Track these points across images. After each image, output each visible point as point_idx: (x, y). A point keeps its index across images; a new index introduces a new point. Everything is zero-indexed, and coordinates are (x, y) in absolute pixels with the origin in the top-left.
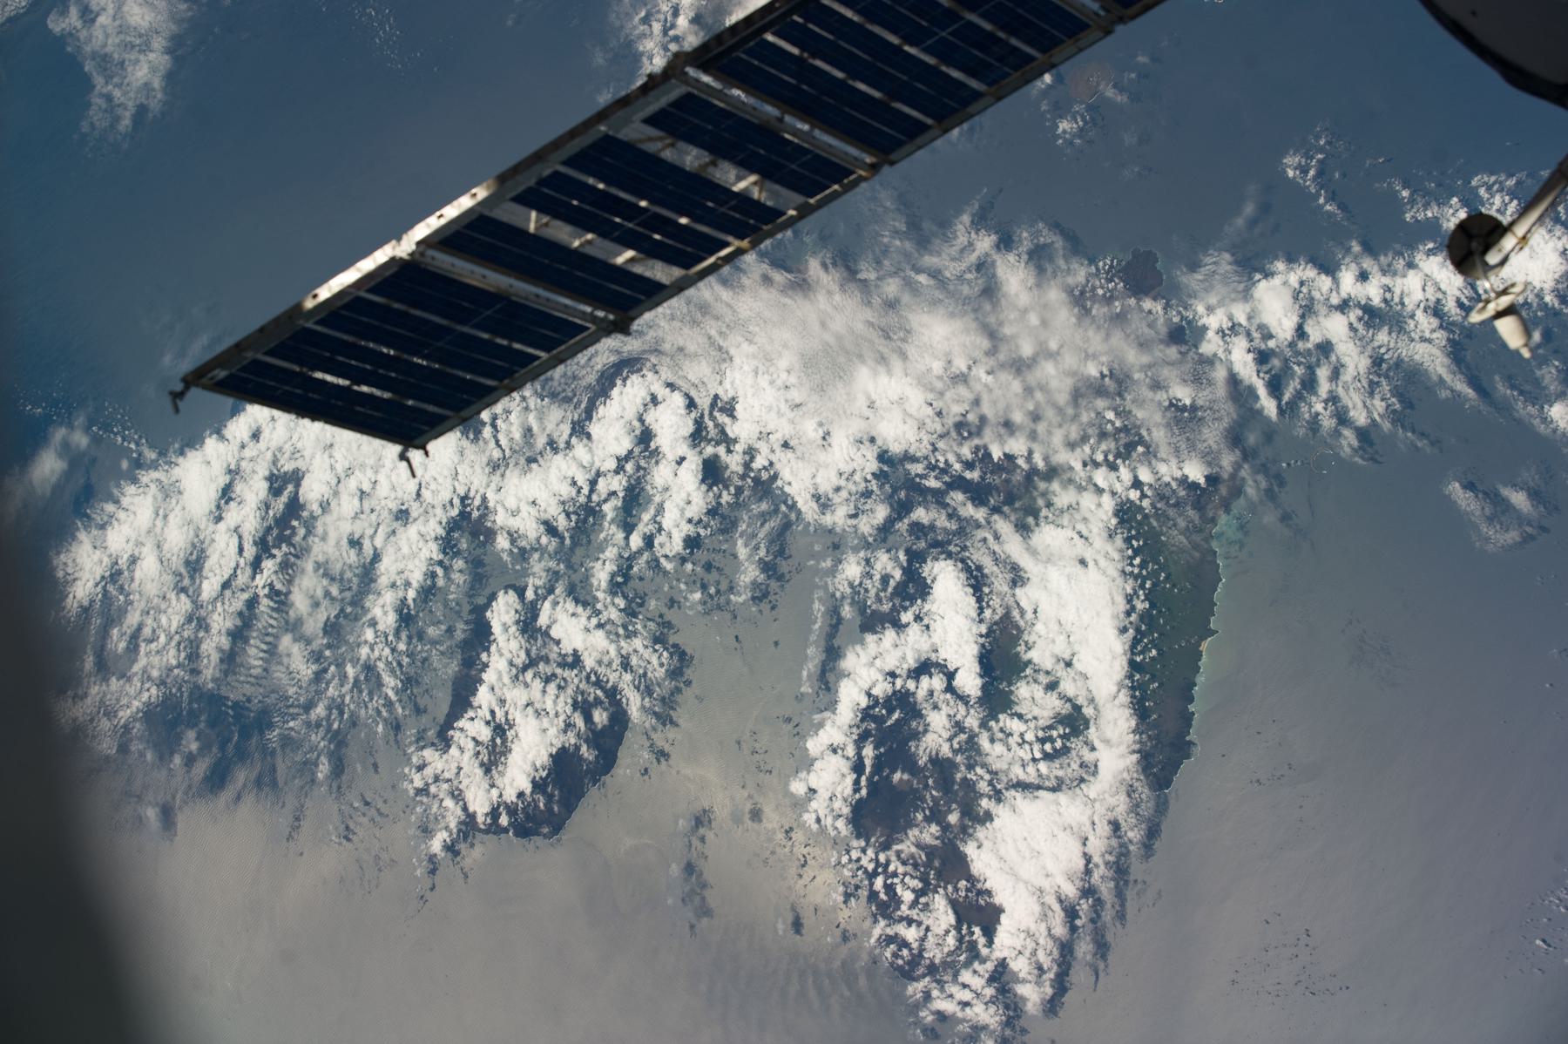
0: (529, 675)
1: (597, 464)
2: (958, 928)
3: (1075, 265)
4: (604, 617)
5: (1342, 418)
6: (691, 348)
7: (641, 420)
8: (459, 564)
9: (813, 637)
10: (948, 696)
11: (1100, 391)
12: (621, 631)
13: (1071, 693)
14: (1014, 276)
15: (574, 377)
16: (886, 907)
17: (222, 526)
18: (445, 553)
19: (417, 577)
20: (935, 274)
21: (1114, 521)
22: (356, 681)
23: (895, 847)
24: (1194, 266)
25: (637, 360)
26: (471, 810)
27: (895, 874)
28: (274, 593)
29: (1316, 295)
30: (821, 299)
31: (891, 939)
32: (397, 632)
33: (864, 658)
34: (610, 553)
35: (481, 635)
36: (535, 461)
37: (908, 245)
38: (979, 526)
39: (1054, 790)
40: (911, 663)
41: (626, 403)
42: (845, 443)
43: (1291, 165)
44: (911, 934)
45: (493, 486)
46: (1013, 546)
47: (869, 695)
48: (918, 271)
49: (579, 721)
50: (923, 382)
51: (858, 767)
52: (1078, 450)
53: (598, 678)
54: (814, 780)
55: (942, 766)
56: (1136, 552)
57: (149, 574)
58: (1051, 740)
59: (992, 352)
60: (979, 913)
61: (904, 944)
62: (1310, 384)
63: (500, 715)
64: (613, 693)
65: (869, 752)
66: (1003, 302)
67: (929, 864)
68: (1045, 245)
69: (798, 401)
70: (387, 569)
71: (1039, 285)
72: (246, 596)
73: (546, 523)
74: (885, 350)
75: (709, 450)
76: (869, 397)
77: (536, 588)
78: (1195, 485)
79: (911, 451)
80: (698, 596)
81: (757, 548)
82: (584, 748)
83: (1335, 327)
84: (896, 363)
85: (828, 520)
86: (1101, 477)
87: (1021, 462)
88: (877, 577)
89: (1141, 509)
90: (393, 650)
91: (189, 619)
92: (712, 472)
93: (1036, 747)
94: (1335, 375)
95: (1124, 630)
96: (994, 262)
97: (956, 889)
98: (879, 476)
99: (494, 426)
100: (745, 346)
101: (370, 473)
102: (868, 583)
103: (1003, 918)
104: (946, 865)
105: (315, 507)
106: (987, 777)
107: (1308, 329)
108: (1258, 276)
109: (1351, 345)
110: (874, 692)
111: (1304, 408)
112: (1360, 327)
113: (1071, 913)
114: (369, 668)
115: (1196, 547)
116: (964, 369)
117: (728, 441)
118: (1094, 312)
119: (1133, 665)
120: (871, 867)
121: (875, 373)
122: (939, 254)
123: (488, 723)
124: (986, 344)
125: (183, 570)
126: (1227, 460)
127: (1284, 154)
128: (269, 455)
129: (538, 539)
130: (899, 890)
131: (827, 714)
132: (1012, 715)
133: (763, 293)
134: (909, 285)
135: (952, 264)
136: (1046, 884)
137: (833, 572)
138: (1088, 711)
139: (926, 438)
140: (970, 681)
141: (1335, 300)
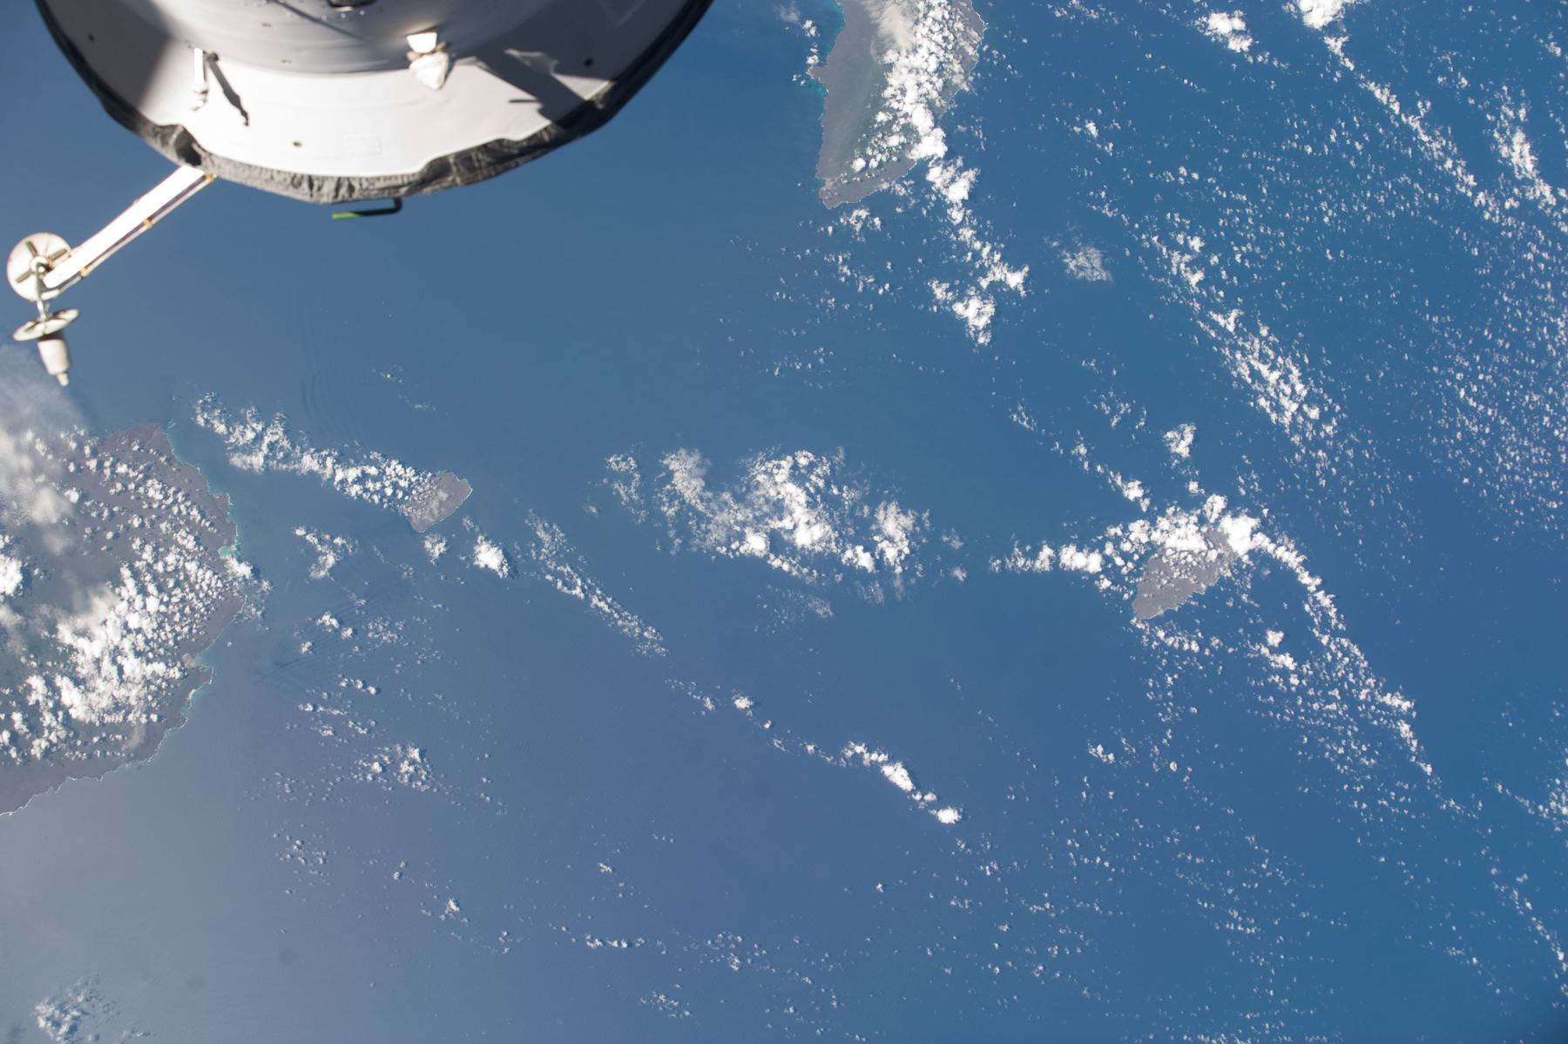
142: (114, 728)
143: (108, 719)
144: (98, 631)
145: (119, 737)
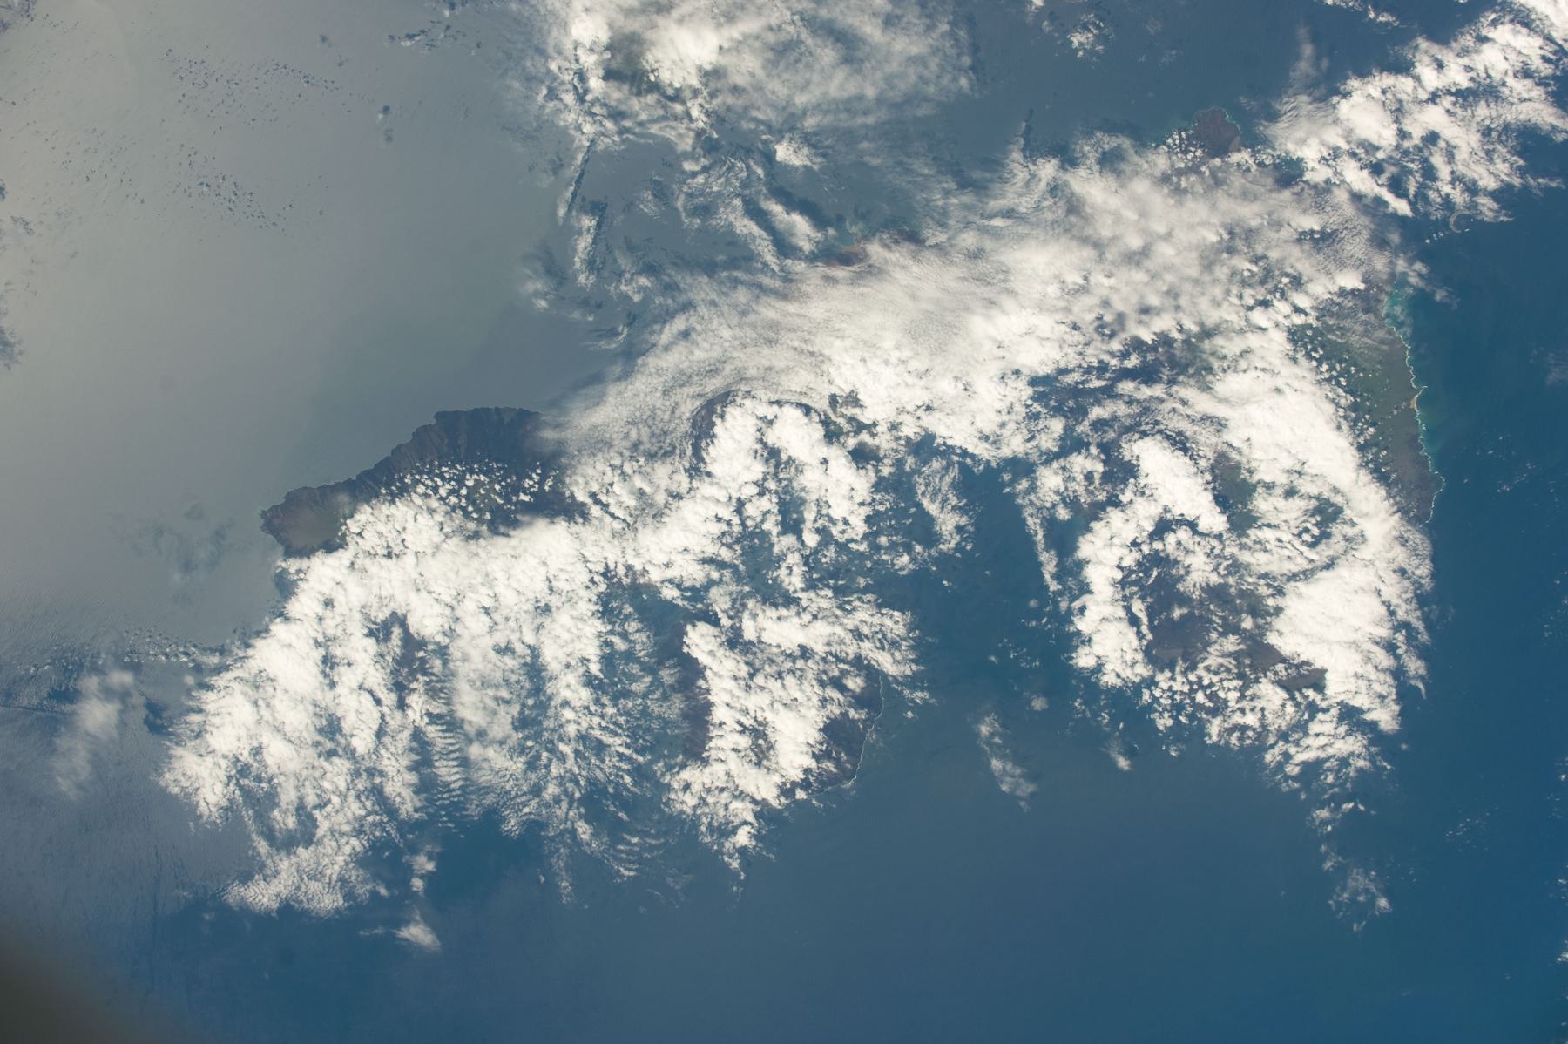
0: (759, 680)
1: (735, 496)
2: (1293, 698)
3: (1152, 157)
4: (814, 608)
5: (1472, 189)
6: (780, 364)
7: (761, 441)
8: (632, 626)
9: (1041, 546)
10: (1197, 539)
11: (1231, 251)
12: (839, 612)
13: (1314, 491)
14: (1091, 186)
15: (665, 433)
16: (1219, 708)
17: (339, 690)
18: (613, 624)
19: (592, 651)
20: (1009, 214)
21: (1290, 347)
22: (577, 753)
23: (1201, 666)
24: (1274, 117)
25: (727, 394)
26: (758, 798)
27: (1211, 685)
28: (434, 718)
29: (1403, 97)
30: (898, 274)
31: (1230, 731)
32: (597, 702)
33: (1099, 542)
34: (793, 559)
35: (691, 671)
37: (967, 198)
38: (1162, 401)
39: (1329, 565)
40: (1149, 527)
41: (737, 437)
44: (1251, 720)
45: (629, 552)
46: (1202, 403)
47: (1119, 567)
48: (991, 217)
49: (835, 694)
50: (1042, 307)
51: (1134, 621)
52: (1225, 304)
53: (836, 656)
54: (1098, 649)
55: (1217, 593)
56: (1320, 362)
57: (280, 755)
58: (1307, 530)
60: (1304, 680)
61: (1243, 728)
62: (1429, 173)
63: (748, 722)
64: (858, 662)
65: (1138, 607)
66: (1088, 210)
67: (1239, 665)
68: (1112, 150)
69: (922, 368)
70: (552, 657)
71: (1123, 186)
72: (406, 734)
73: (704, 561)
74: (991, 296)
75: (852, 442)
76: (995, 340)
77: (725, 612)
78: (1354, 293)
79: (1062, 365)
80: (905, 559)
81: (945, 501)
82: (852, 713)
83: (1435, 118)
84: (1008, 303)
85: (1006, 452)
86: (1259, 317)
87: (1176, 335)
88: (1080, 478)
89: (1310, 327)
90: (602, 716)
91: (356, 774)
92: (862, 456)
93: (1297, 543)
94: (1450, 155)
95: (1339, 428)
96: (1066, 184)
97: (1276, 673)
98: (1037, 398)
99: (598, 502)
100: (838, 343)
101: (484, 590)
102: (1072, 485)
103: (1327, 676)
104: (1258, 657)
105: (439, 638)
106: (1262, 582)
107: (1407, 128)
108: (1335, 99)
109: (1456, 129)
110: (1124, 564)
111: (1432, 195)
112: (1458, 110)
113: (1390, 647)
114: (583, 737)
115: (1382, 342)
116: (1081, 282)
117: (871, 428)
118: (1184, 184)
119: (1361, 448)
120: (1186, 689)
121: (988, 317)
122: (1003, 196)
123: (741, 732)
124: (1088, 253)
125: (319, 738)
126: (1380, 263)
128: (357, 616)
129: (708, 576)
130: (1221, 694)
131: (1086, 598)
132: (1260, 527)
133: (831, 291)
134: (983, 231)
135: (1023, 200)
136: (1352, 636)
137: (1032, 489)
138: (1338, 500)
139: (1070, 351)
140: (1213, 520)
141: (1423, 96)
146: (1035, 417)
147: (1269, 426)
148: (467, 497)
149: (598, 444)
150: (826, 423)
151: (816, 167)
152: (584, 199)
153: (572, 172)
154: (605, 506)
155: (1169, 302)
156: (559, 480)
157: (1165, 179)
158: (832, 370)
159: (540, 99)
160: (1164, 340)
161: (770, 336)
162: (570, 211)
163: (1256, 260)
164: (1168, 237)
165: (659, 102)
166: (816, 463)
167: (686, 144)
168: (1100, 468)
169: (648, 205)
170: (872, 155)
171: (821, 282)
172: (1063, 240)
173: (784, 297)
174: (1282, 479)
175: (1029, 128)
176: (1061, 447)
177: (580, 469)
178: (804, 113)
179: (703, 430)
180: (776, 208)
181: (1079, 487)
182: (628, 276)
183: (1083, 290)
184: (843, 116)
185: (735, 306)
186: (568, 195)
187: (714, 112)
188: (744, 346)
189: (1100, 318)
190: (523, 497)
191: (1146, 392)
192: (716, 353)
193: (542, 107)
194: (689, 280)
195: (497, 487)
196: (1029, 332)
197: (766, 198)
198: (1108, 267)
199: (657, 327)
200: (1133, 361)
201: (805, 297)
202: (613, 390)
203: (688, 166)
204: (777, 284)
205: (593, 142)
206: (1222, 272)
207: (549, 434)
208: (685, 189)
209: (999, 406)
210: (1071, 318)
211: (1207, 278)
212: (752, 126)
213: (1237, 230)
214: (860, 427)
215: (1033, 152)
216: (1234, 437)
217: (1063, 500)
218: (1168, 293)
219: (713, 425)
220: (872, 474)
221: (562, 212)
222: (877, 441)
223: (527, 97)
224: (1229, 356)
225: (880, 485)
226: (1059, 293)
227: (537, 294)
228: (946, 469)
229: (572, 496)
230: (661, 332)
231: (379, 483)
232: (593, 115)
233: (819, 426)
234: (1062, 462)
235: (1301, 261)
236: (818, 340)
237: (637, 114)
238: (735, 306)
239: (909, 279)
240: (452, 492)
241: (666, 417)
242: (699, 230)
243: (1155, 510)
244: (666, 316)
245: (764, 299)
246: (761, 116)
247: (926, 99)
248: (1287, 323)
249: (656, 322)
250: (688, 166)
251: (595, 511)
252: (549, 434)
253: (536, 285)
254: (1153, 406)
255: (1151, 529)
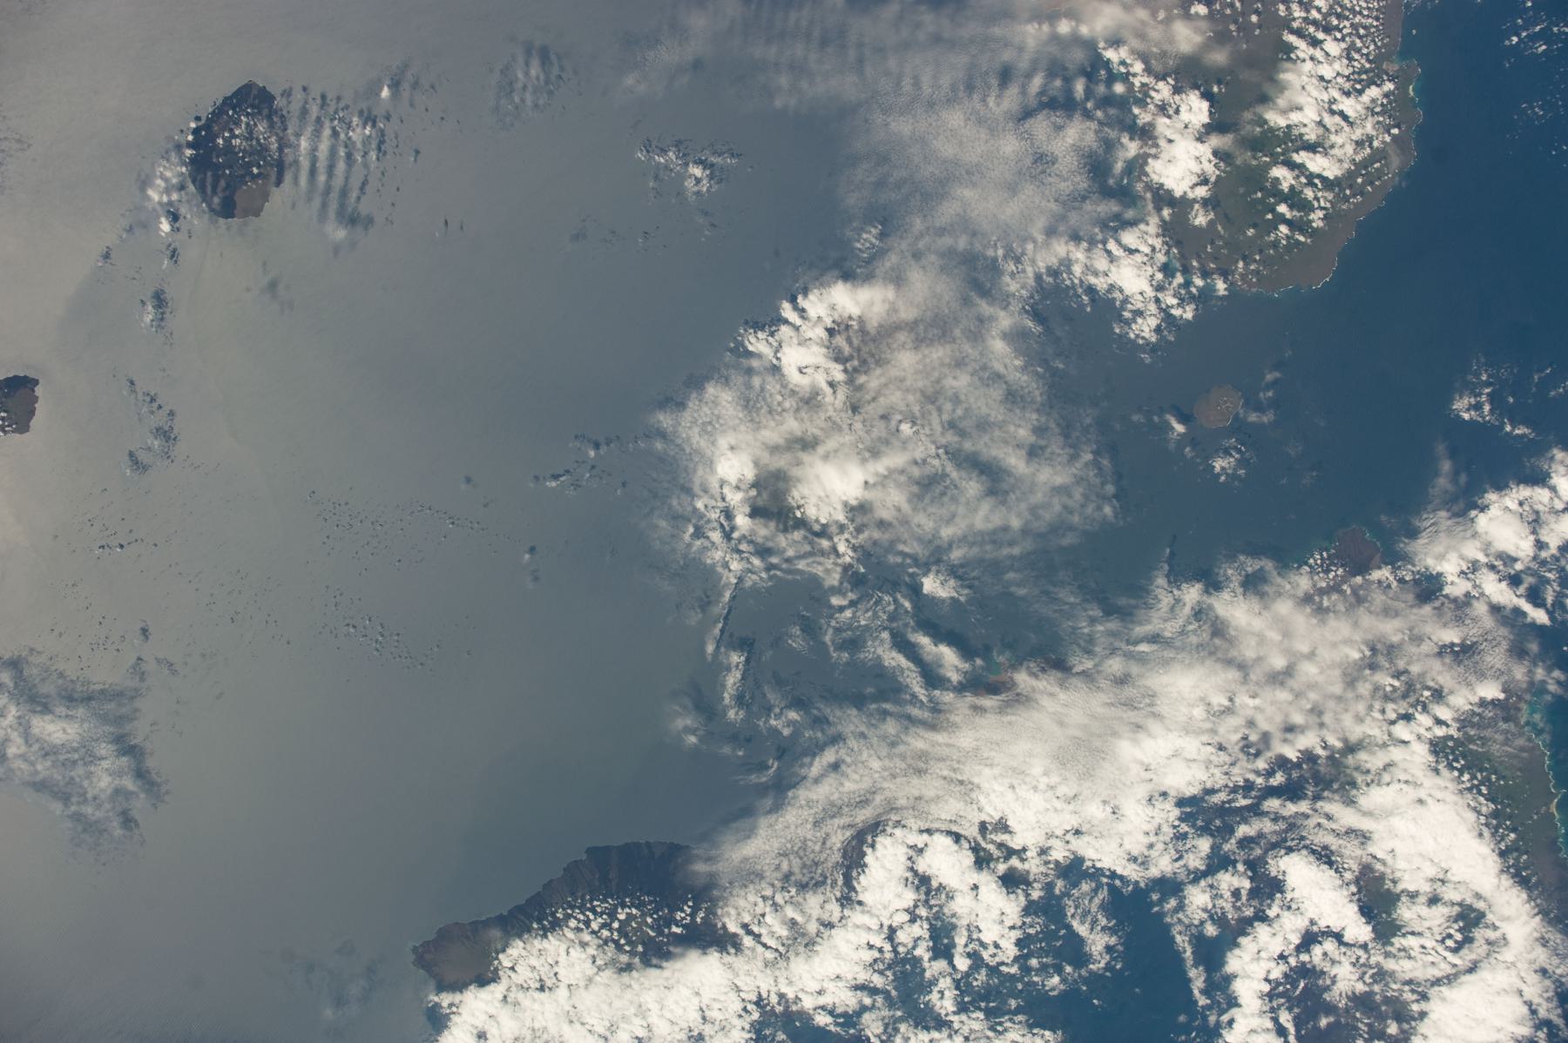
1: (886, 923)
3: (1294, 578)
6: (929, 793)
7: (912, 869)
11: (1373, 667)
13: (1456, 897)
14: (1235, 610)
15: (816, 864)
20: (1154, 639)
21: (1432, 758)
24: (1413, 534)
25: (877, 824)
30: (1046, 702)
36: (814, 943)
37: (1113, 625)
38: (1307, 816)
41: (888, 865)
42: (1140, 809)
43: (1462, 406)
46: (1347, 818)
48: (1136, 643)
50: (1187, 729)
58: (1450, 936)
59: (1245, 680)
71: (1266, 608)
74: (1139, 720)
75: (1002, 868)
79: (1209, 785)
81: (1094, 922)
85: (1154, 872)
86: (1401, 731)
88: (1227, 895)
92: (1011, 881)
93: (1440, 949)
96: (1210, 607)
99: (750, 932)
100: (987, 771)
102: (1220, 903)
108: (1473, 513)
116: (1226, 703)
117: (1020, 853)
118: (1326, 603)
121: (1135, 741)
122: (1149, 621)
124: (1233, 674)
127: (1451, 401)
132: (1404, 935)
134: (1129, 656)
135: (1168, 625)
137: (1181, 907)
140: (1358, 930)
142: (1365, 163)
143: (1358, 158)
144: (1301, 99)
145: (1377, 165)
146: (1183, 837)
147: (1413, 837)
148: (618, 930)
149: (750, 876)
150: (976, 849)
151: (962, 599)
152: (731, 635)
153: (719, 609)
154: (757, 937)
155: (1313, 719)
156: (711, 912)
157: (1307, 599)
158: (981, 798)
159: (687, 537)
160: (1309, 757)
161: (919, 766)
162: (718, 647)
163: (1397, 675)
164: (1311, 656)
165: (805, 538)
166: (966, 889)
167: (834, 579)
168: (1247, 884)
169: (797, 640)
170: (1019, 585)
171: (968, 712)
172: (1208, 662)
173: (933, 727)
174: (1426, 888)
175: (1172, 554)
176: (1208, 866)
177: (732, 901)
178: (950, 545)
179: (853, 860)
180: (924, 641)
181: (1226, 904)
182: (777, 710)
183: (1228, 711)
184: (988, 547)
185: (884, 738)
186: (717, 631)
187: (861, 547)
188: (894, 776)
189: (1245, 738)
190: (675, 929)
191: (1291, 808)
192: (866, 784)
193: (689, 545)
194: (838, 713)
195: (649, 920)
196: (1176, 754)
197: (914, 631)
198: (1253, 688)
199: (807, 760)
200: (1278, 779)
201: (955, 726)
202: (763, 822)
203: (836, 601)
204: (926, 715)
205: (740, 579)
206: (1364, 688)
207: (700, 867)
208: (833, 623)
209: (1146, 827)
210: (1217, 739)
211: (1350, 695)
212: (899, 560)
213: (1379, 646)
214: (1010, 853)
215: (1177, 577)
216: (1378, 849)
217: (1211, 917)
218: (1312, 710)
219: (864, 854)
220: (1022, 899)
221: (710, 648)
222: (1026, 866)
223: (673, 536)
224: (1373, 770)
225: (1029, 909)
226: (1205, 715)
227: (687, 730)
228: (1095, 891)
229: (724, 927)
230: (811, 764)
231: (531, 918)
232: (739, 552)
233: (969, 853)
234: (1209, 880)
235: (1441, 674)
236: (967, 769)
237: (784, 551)
238: (884, 738)
239: (1056, 706)
240: (603, 926)
241: (817, 848)
242: (847, 664)
243: (1301, 923)
244: (817, 749)
245: (913, 730)
246: (907, 550)
247: (1071, 528)
248: (1429, 735)
249: (806, 755)
250: (836, 601)
251: (748, 941)
252: (700, 867)
253: (684, 721)
254: (1299, 822)
255: (1297, 941)
